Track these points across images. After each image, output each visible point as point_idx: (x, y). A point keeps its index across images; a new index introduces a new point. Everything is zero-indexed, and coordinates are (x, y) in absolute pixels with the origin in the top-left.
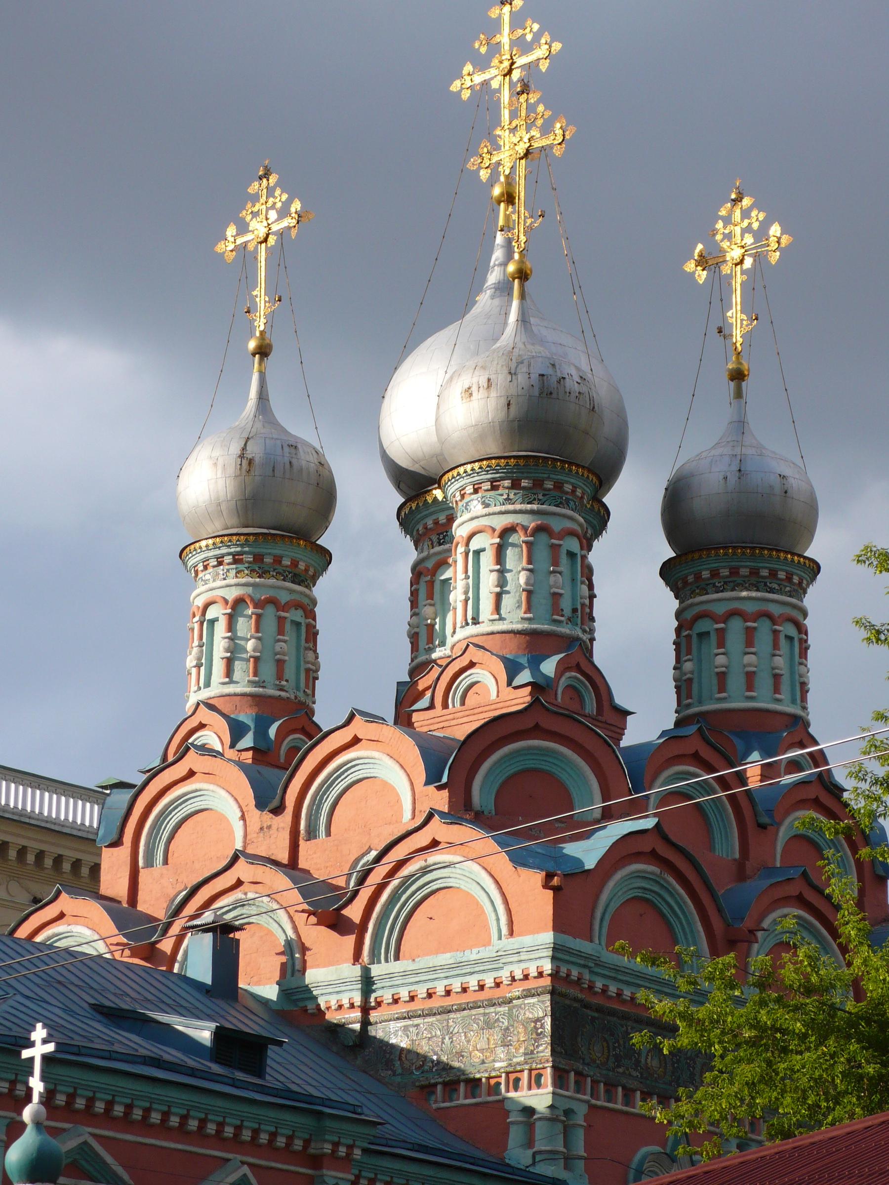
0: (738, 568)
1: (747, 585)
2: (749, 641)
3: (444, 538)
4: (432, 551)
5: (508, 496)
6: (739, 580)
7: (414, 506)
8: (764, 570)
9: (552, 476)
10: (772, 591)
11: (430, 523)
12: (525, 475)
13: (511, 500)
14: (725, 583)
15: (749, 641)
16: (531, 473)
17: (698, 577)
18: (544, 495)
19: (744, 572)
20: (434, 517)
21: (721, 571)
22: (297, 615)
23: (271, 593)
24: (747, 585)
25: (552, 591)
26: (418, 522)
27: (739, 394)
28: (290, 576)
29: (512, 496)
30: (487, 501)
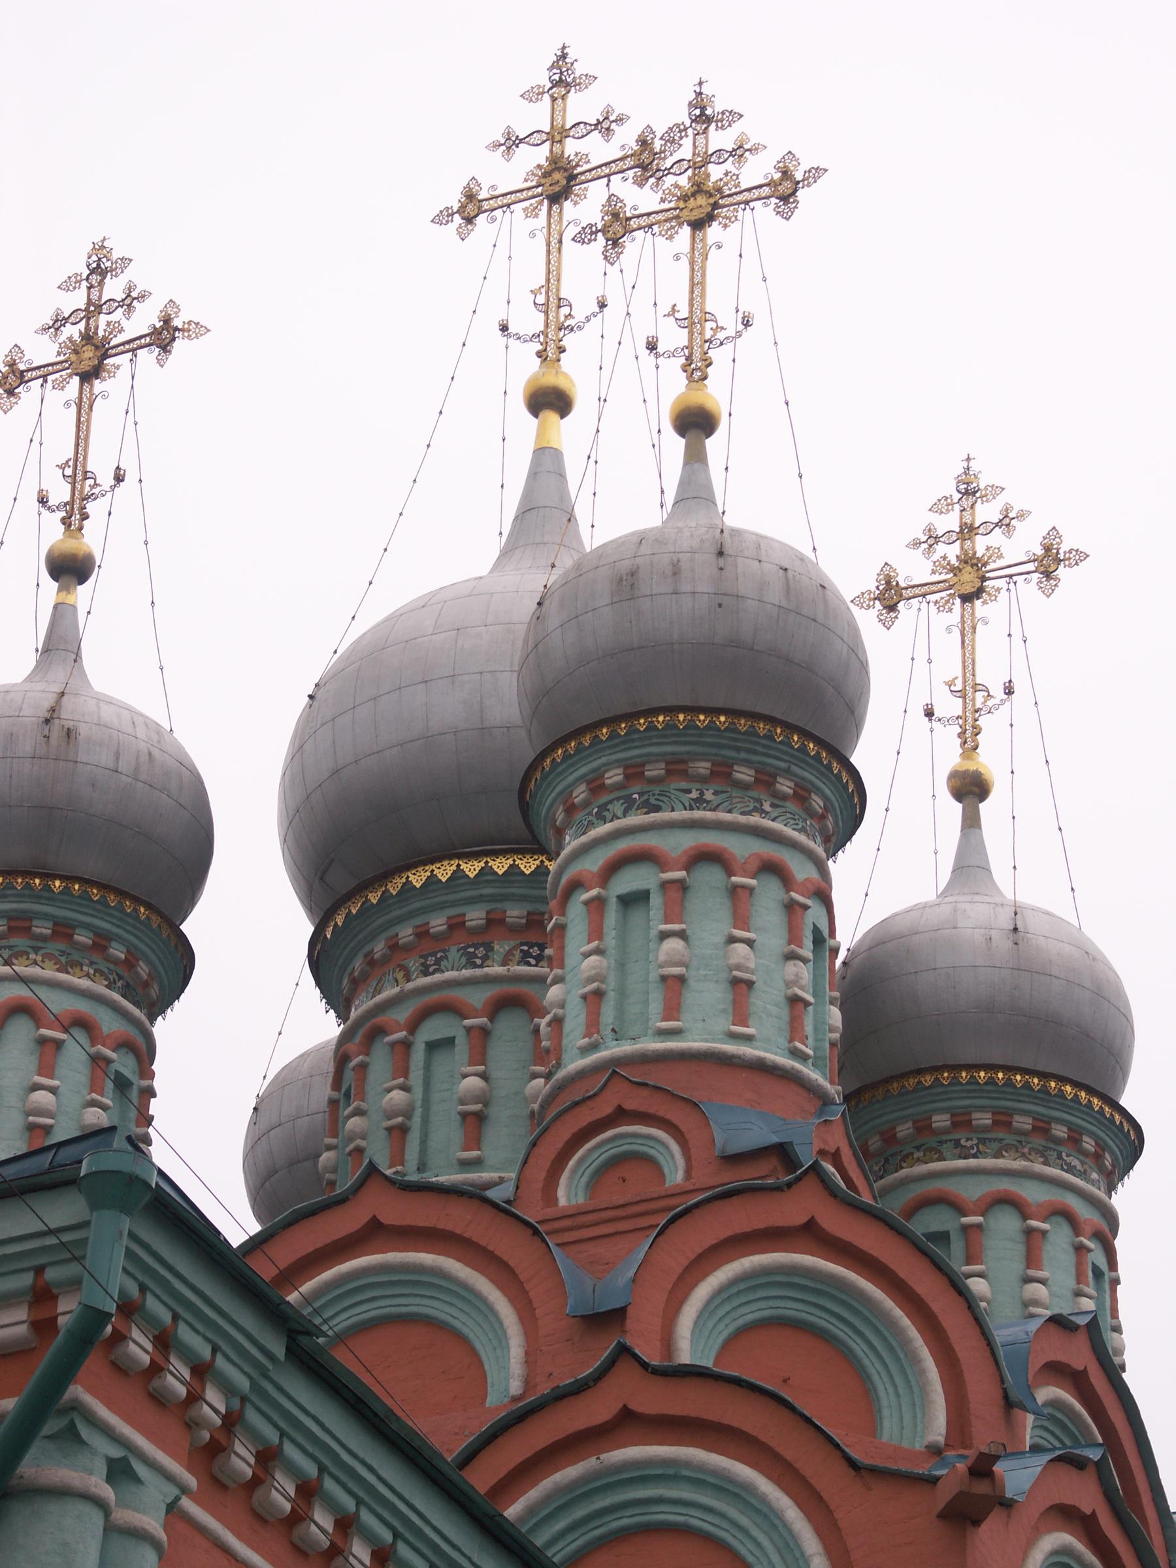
0: (1010, 1113)
1: (1026, 1150)
2: (1032, 1258)
3: (438, 962)
4: (410, 986)
5: (702, 794)
6: (1010, 1139)
7: (374, 898)
8: (1058, 1127)
9: (794, 768)
10: (1070, 1169)
11: (406, 933)
12: (743, 755)
13: (708, 802)
14: (982, 1141)
15: (1032, 1258)
16: (755, 752)
17: (923, 1127)
18: (773, 805)
19: (1023, 1122)
20: (418, 921)
21: (975, 1115)
22: (124, 1064)
23: (83, 1006)
24: (1026, 1150)
25: (790, 992)
26: (373, 936)
27: (971, 821)
28: (119, 984)
29: (708, 795)
30: (653, 801)
